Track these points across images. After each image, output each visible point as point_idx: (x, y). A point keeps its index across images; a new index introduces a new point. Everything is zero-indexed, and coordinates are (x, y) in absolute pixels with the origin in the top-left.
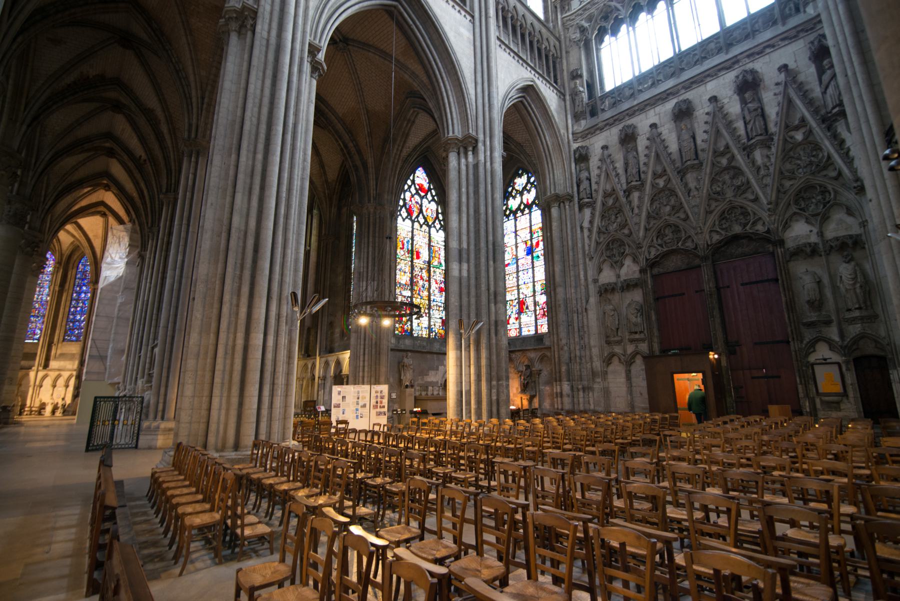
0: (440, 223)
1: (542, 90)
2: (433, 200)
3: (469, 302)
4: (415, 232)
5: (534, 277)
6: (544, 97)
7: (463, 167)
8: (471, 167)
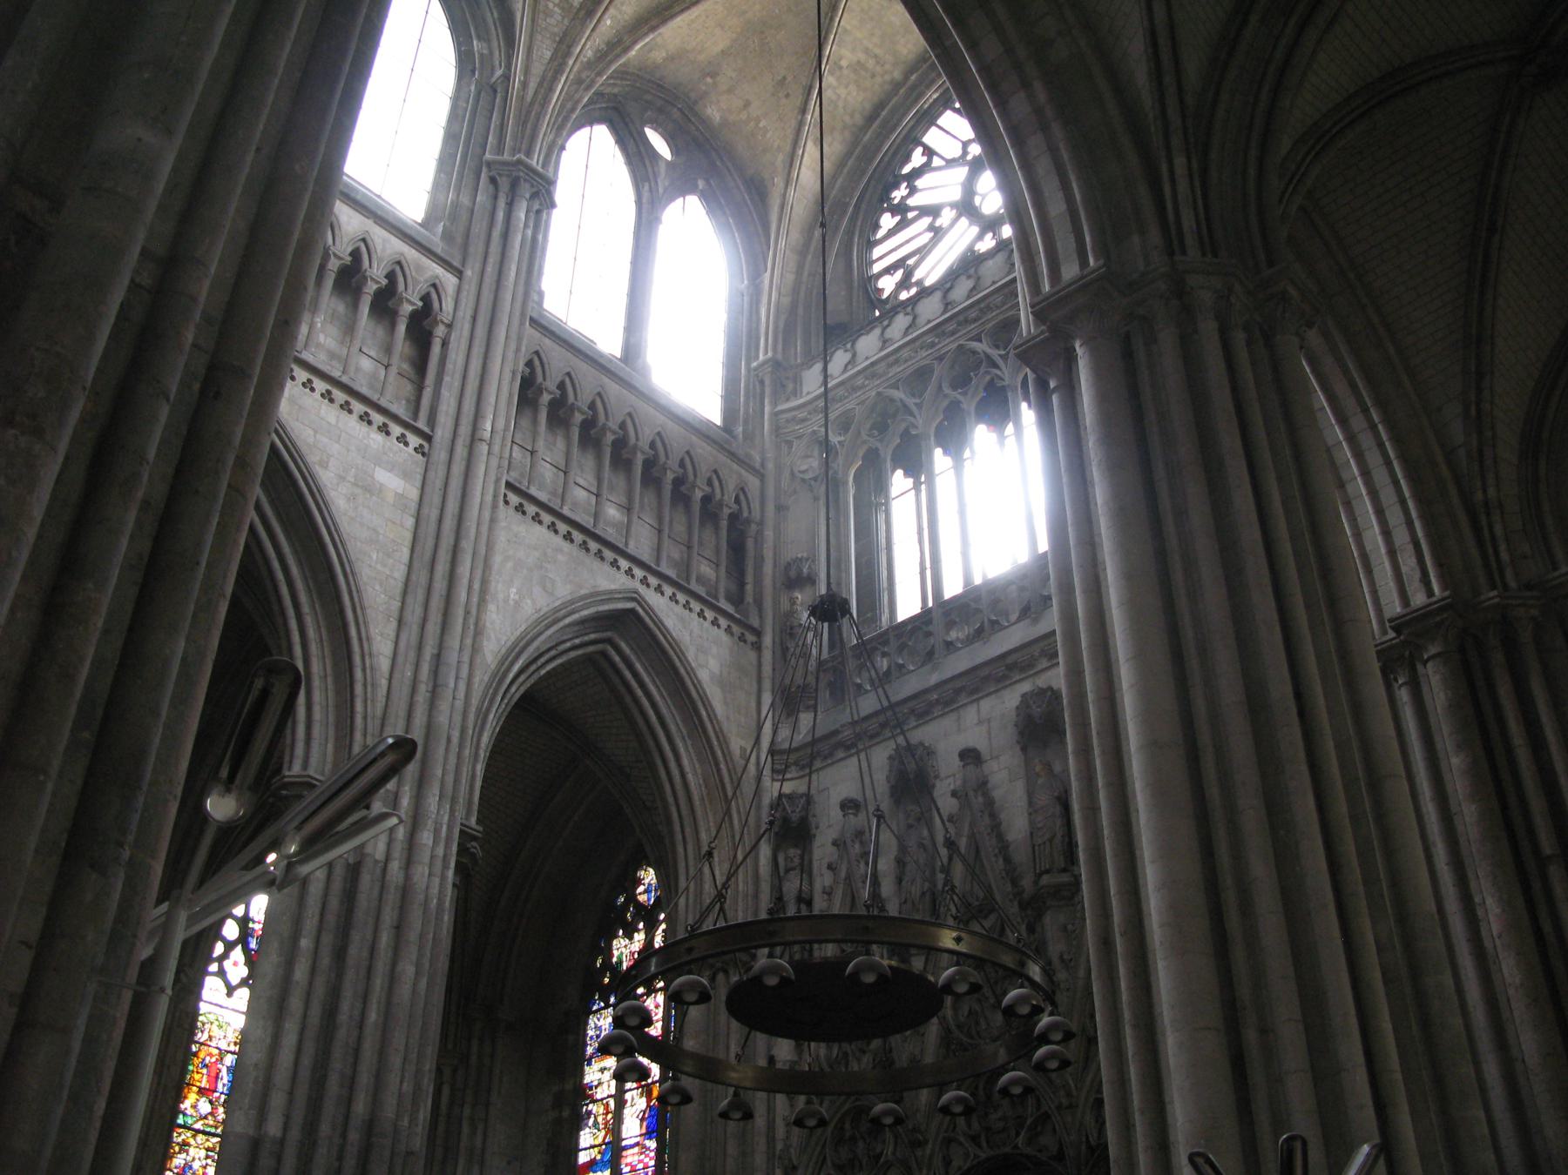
1: (670, 623)
6: (675, 644)
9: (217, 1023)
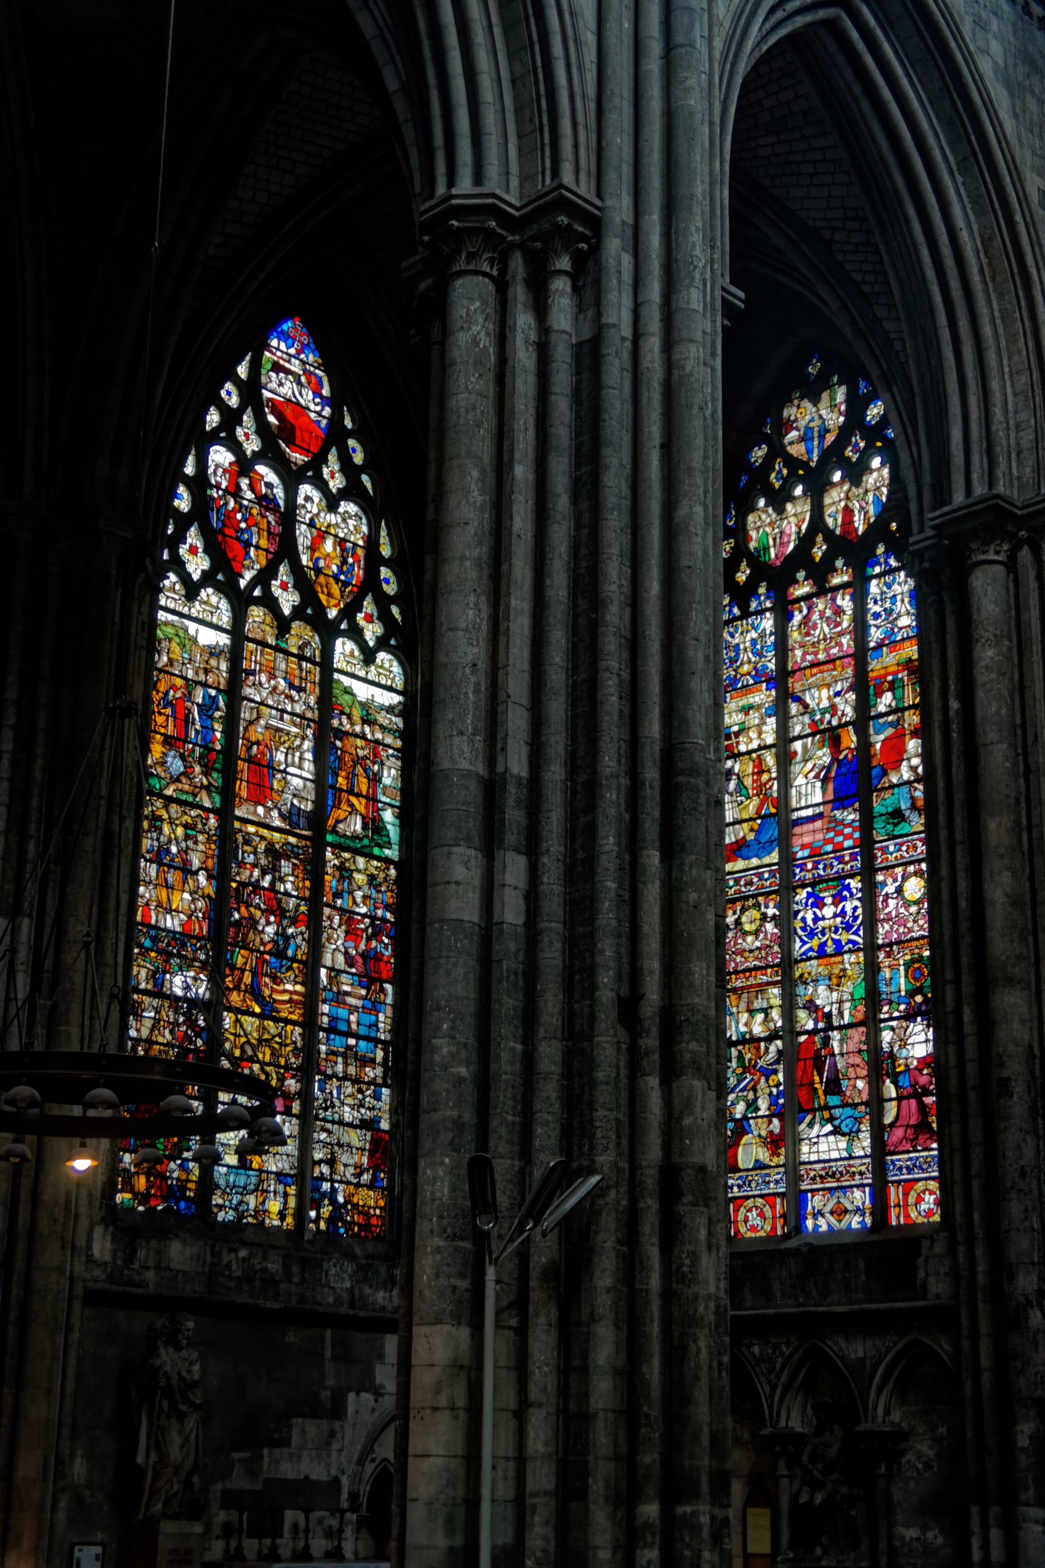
0: (385, 616)
2: (352, 491)
3: (529, 1059)
4: (253, 656)
5: (871, 921)
7: (524, 357)
8: (562, 355)
9: (177, 640)
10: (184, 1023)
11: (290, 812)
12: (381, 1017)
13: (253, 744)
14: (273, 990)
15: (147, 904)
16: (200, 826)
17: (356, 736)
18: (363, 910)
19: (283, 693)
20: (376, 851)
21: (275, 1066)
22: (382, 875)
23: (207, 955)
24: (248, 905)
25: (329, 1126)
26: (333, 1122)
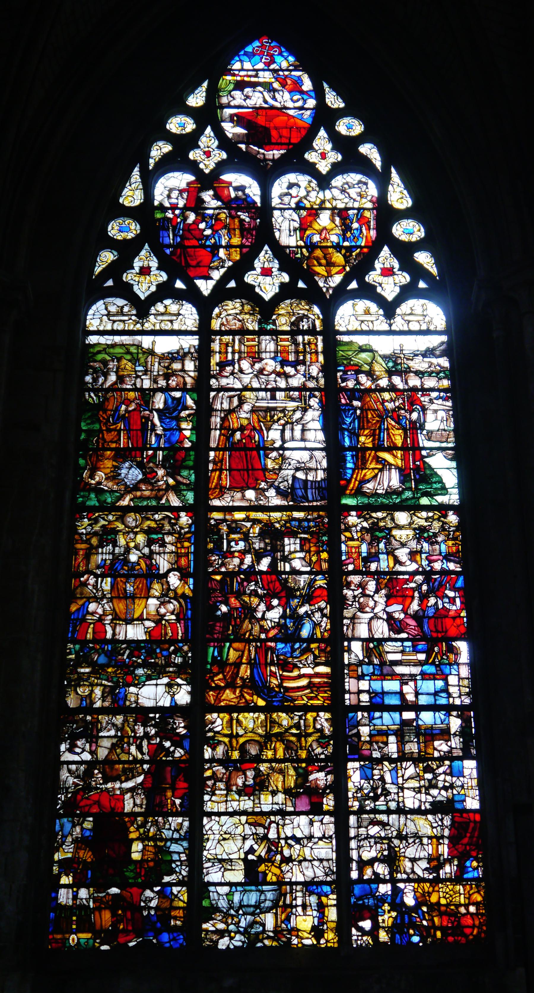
9: (128, 357)
10: (156, 735)
11: (293, 487)
12: (453, 680)
13: (234, 431)
14: (283, 678)
15: (101, 619)
16: (167, 527)
17: (383, 390)
18: (413, 567)
19: (274, 372)
20: (424, 501)
21: (292, 761)
22: (436, 525)
23: (184, 657)
24: (239, 595)
25: (383, 818)
26: (389, 812)
